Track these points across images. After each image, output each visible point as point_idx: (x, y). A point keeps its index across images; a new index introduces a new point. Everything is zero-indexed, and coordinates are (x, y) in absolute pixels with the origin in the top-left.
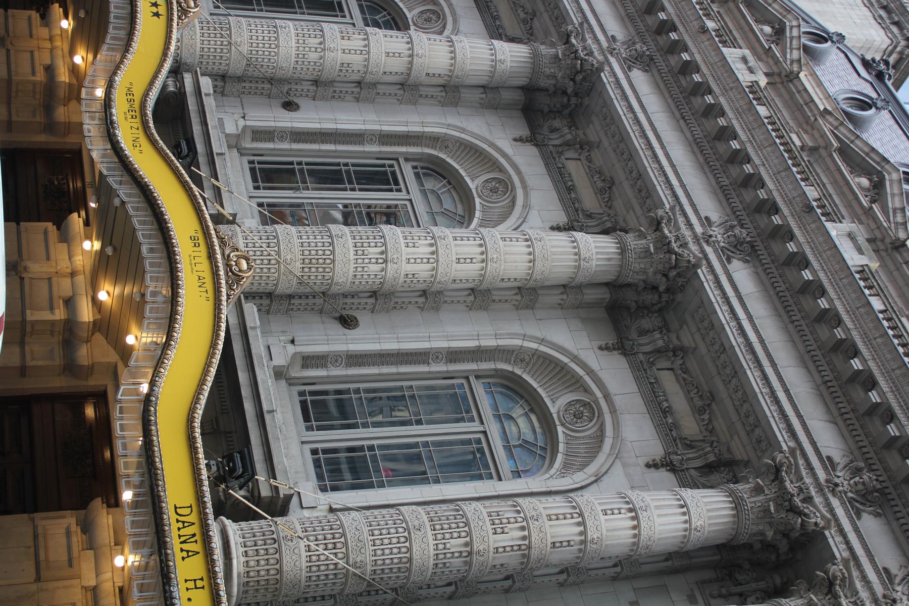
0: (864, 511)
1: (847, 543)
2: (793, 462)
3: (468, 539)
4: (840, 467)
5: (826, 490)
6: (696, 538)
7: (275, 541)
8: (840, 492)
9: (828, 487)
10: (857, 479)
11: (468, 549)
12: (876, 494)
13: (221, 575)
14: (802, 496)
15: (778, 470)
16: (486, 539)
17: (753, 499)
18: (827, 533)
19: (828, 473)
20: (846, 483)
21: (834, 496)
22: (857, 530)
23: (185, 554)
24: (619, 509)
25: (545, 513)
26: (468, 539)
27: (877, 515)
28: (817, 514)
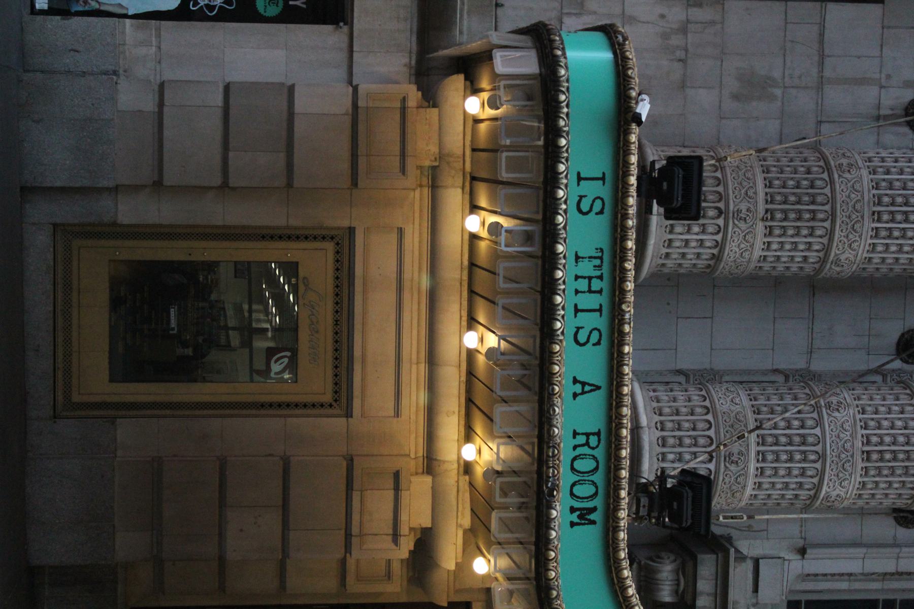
7: (720, 212)
13: (631, 255)
23: (578, 388)
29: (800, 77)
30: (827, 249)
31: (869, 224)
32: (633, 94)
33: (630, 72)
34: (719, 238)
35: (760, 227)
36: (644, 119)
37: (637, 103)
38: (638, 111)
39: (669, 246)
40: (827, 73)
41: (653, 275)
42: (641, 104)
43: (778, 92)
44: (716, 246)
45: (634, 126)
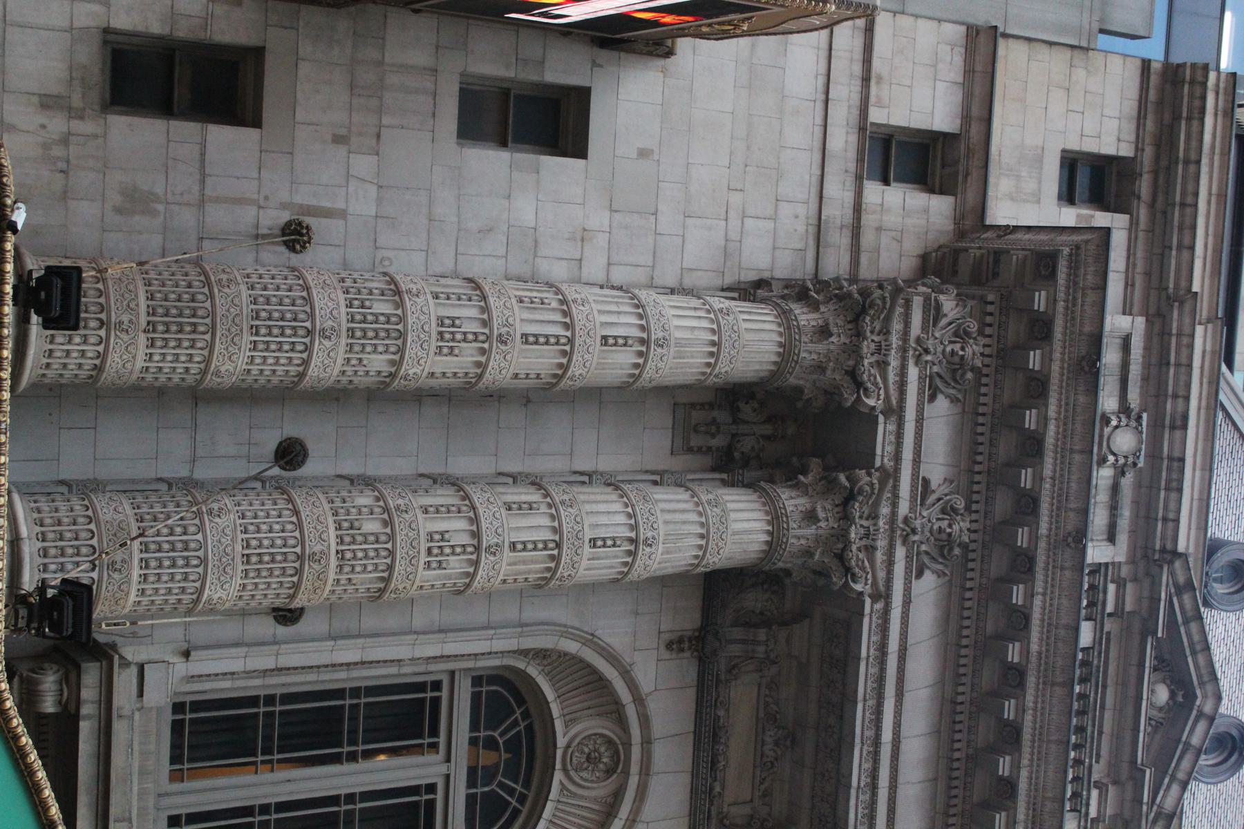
0: (942, 392)
1: (899, 435)
2: (888, 306)
3: (397, 357)
4: (944, 322)
5: (911, 353)
6: (711, 380)
7: (102, 323)
8: (927, 362)
9: (915, 350)
10: (957, 347)
11: (393, 370)
12: (969, 375)
14: (873, 359)
15: (863, 311)
16: (422, 362)
17: (811, 347)
18: (881, 418)
19: (924, 328)
20: (940, 349)
21: (916, 364)
22: (920, 420)
24: (626, 338)
25: (521, 328)
26: (397, 357)
27: (954, 400)
28: (882, 392)
29: (182, 194)
30: (207, 361)
31: (247, 338)
32: (9, 202)
33: (5, 180)
34: (101, 348)
35: (142, 339)
36: (19, 227)
37: (12, 211)
38: (13, 219)
39: (50, 356)
40: (208, 192)
41: (34, 386)
42: (16, 212)
43: (160, 207)
44: (98, 357)
45: (9, 234)
